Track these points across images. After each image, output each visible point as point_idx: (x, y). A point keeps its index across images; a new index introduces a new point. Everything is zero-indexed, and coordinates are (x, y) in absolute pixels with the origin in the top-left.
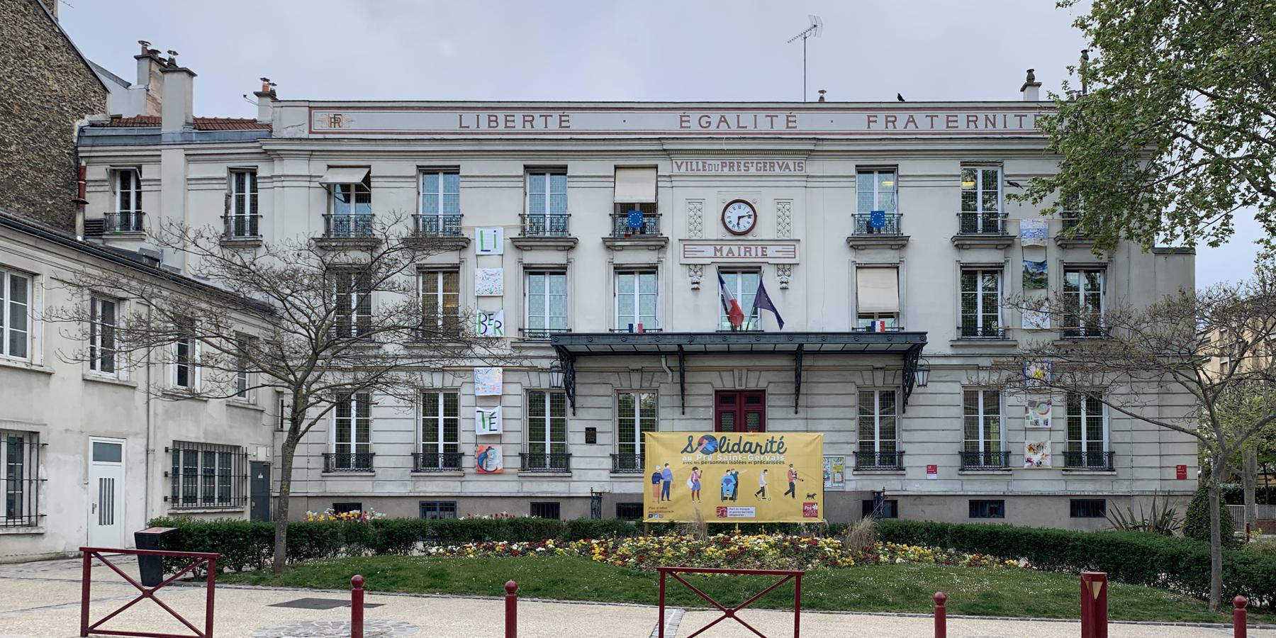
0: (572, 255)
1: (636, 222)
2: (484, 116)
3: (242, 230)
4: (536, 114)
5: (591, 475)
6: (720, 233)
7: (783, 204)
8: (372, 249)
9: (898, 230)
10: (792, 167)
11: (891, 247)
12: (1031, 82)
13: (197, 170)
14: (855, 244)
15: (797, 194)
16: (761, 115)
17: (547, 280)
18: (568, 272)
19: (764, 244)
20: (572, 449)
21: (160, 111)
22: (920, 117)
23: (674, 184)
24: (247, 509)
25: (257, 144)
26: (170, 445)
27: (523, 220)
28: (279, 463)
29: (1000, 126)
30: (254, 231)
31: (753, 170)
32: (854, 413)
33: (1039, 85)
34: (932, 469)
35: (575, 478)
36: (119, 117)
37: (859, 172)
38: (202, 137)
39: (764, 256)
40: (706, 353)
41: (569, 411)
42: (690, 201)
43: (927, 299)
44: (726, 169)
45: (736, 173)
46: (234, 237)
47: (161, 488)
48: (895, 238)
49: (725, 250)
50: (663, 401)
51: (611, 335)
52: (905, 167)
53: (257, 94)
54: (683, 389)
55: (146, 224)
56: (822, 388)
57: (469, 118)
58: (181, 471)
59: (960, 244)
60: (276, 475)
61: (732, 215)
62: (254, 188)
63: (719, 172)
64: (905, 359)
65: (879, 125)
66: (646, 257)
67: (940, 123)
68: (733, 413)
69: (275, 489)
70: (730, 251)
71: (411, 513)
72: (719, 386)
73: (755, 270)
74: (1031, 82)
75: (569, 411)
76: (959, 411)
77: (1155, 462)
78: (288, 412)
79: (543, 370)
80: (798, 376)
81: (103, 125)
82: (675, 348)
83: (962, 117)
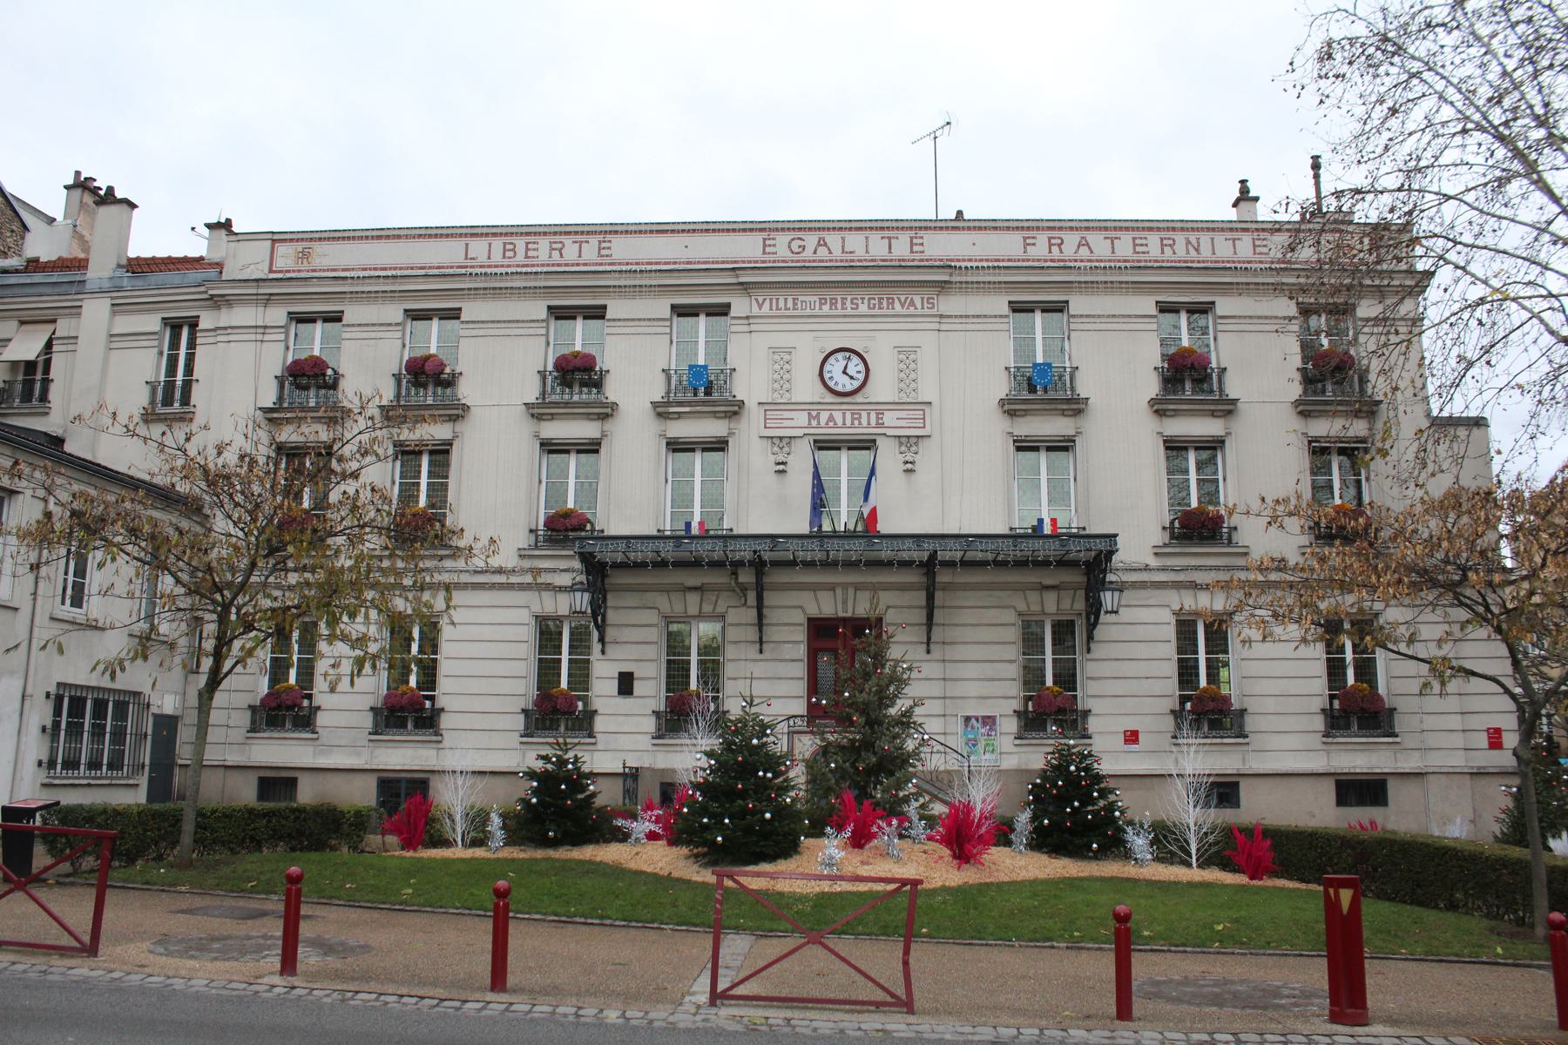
0: (608, 425)
1: (703, 391)
2: (498, 244)
3: (172, 399)
4: (568, 240)
5: (625, 742)
6: (818, 393)
7: (907, 356)
8: (331, 421)
9: (1073, 389)
10: (919, 305)
11: (1063, 413)
12: (1245, 196)
13: (126, 323)
14: (1011, 408)
15: (926, 341)
16: (875, 237)
17: (573, 460)
18: (603, 450)
19: (880, 408)
20: (597, 704)
21: (86, 250)
22: (1096, 239)
23: (753, 327)
24: (143, 781)
25: (202, 289)
26: (53, 690)
27: (544, 379)
28: (192, 717)
29: (1206, 252)
30: (186, 400)
31: (863, 308)
32: (1013, 652)
33: (1256, 199)
34: (1132, 737)
35: (599, 747)
36: (36, 260)
37: (1015, 311)
38: (139, 283)
39: (880, 425)
40: (793, 563)
41: (596, 647)
42: (774, 350)
43: (1121, 487)
44: (826, 308)
45: (840, 312)
46: (160, 410)
47: (36, 747)
48: (1068, 401)
49: (824, 416)
50: (732, 633)
51: (660, 537)
52: (1078, 304)
53: (209, 226)
54: (760, 616)
55: (52, 396)
56: (969, 616)
57: (478, 248)
58: (63, 726)
59: (1160, 408)
60: (185, 734)
61: (835, 367)
62: (192, 344)
63: (817, 311)
64: (1087, 574)
65: (1040, 249)
66: (710, 428)
67: (1124, 247)
68: (834, 651)
69: (184, 753)
70: (831, 418)
71: (363, 795)
72: (813, 611)
73: (867, 444)
74: (1245, 196)
75: (596, 647)
76: (1170, 650)
77: (1455, 722)
78: (209, 645)
79: (562, 589)
80: (930, 598)
81: (17, 271)
82: (748, 556)
83: (1153, 240)
